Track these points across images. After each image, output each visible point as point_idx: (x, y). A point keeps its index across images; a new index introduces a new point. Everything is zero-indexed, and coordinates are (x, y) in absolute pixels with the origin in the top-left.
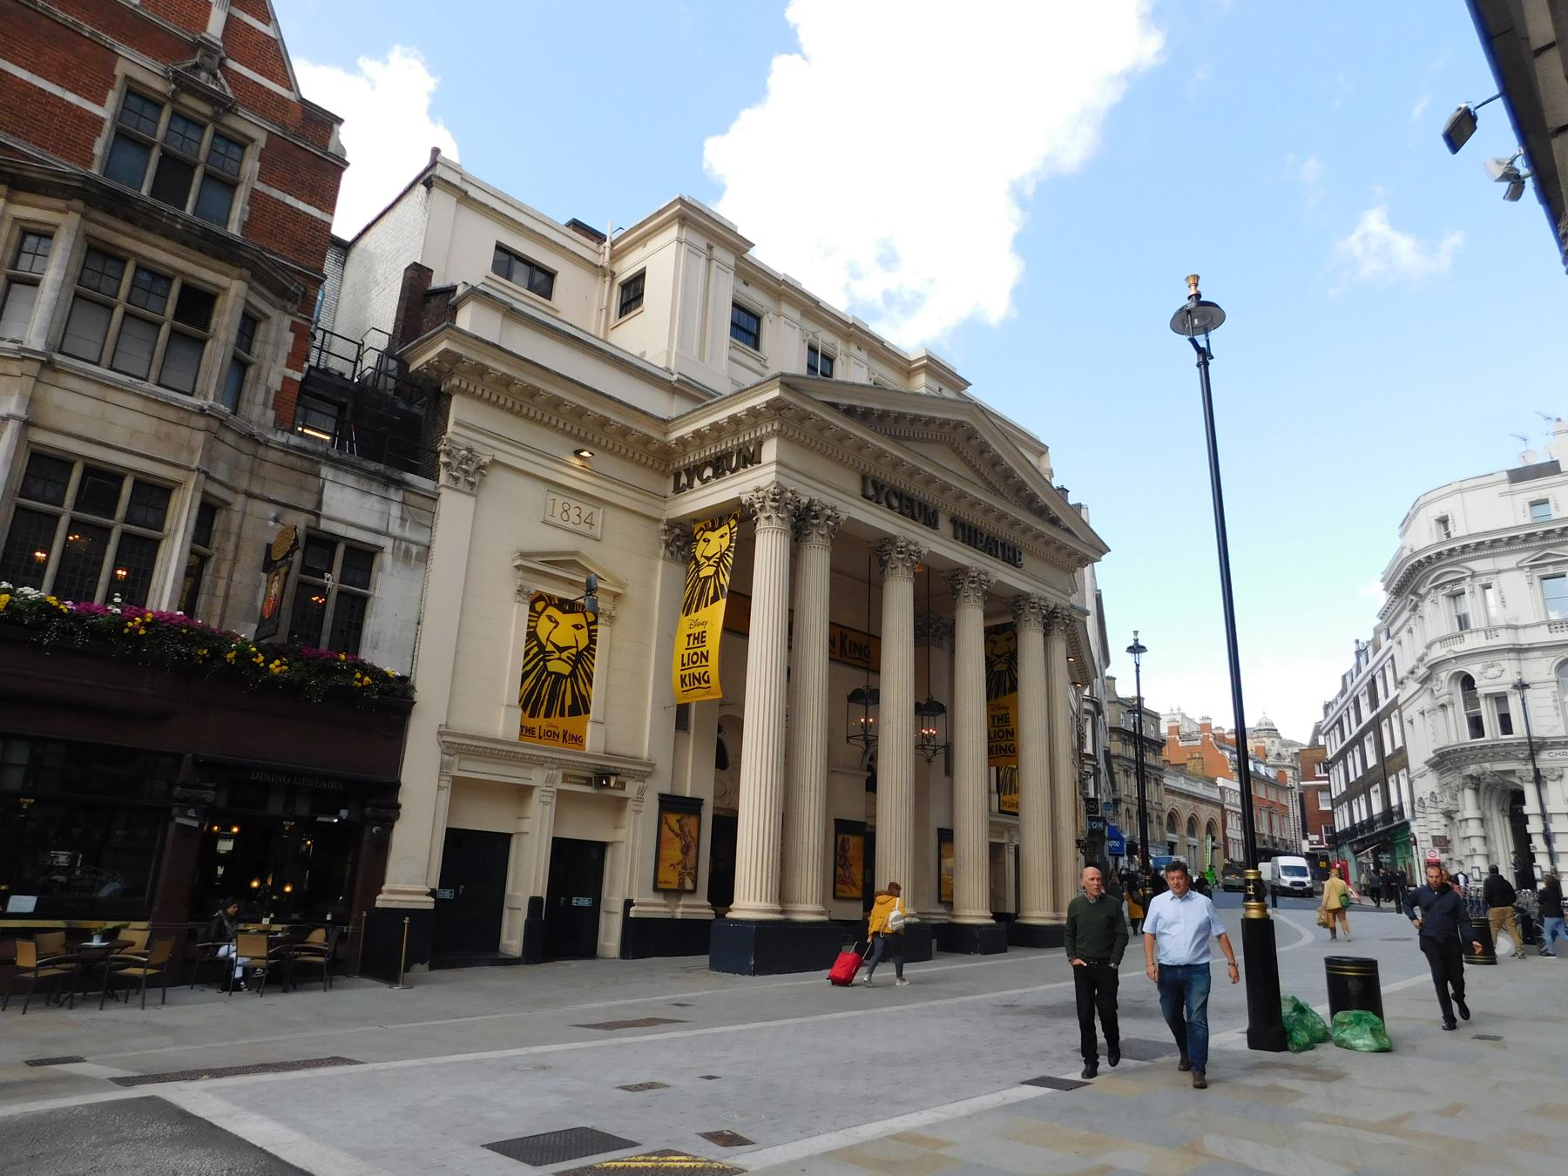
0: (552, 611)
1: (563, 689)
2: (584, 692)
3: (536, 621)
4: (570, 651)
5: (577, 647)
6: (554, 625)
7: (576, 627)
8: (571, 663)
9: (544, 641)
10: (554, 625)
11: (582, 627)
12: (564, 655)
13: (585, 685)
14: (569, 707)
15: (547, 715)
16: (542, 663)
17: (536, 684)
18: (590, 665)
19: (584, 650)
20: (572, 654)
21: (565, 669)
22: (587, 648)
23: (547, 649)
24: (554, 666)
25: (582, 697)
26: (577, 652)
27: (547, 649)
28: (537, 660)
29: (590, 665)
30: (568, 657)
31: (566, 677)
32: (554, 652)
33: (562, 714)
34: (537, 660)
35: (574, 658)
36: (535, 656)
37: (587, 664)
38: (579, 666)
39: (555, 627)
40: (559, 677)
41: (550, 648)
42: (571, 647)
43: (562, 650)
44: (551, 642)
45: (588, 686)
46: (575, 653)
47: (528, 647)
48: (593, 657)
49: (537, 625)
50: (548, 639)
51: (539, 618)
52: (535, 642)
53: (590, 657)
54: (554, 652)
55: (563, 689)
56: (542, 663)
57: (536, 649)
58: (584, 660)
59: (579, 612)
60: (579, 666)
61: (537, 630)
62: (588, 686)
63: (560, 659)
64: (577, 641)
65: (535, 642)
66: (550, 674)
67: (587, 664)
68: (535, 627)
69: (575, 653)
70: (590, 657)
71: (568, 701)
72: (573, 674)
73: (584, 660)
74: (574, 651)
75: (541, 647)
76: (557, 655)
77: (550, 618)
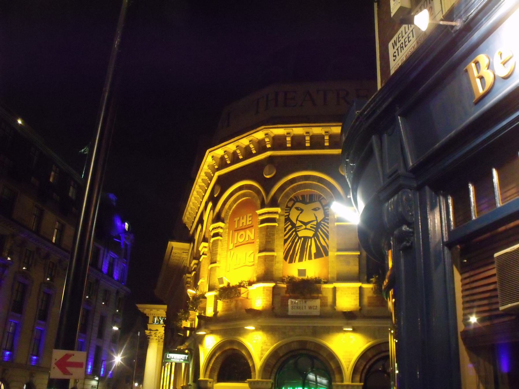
0: (298, 205)
1: (309, 244)
2: (323, 243)
3: (289, 212)
4: (312, 223)
5: (317, 220)
6: (301, 211)
7: (315, 209)
8: (313, 229)
9: (294, 221)
10: (301, 211)
11: (319, 209)
12: (308, 226)
13: (324, 240)
14: (315, 254)
15: (301, 260)
16: (294, 233)
17: (292, 245)
18: (326, 228)
19: (321, 221)
20: (314, 225)
21: (310, 234)
22: (324, 220)
23: (297, 225)
24: (300, 234)
25: (323, 247)
26: (317, 223)
27: (297, 225)
28: (291, 232)
29: (326, 228)
30: (311, 227)
31: (311, 238)
32: (302, 226)
33: (310, 258)
34: (291, 232)
35: (315, 227)
36: (290, 230)
37: (324, 228)
38: (319, 230)
39: (301, 213)
40: (306, 238)
41: (299, 224)
42: (314, 221)
43: (306, 224)
44: (300, 221)
45: (326, 240)
46: (315, 224)
47: (286, 226)
48: (328, 223)
49: (289, 214)
50: (297, 220)
51: (290, 210)
52: (289, 223)
53: (326, 224)
54: (302, 226)
55: (309, 244)
56: (294, 233)
57: (290, 227)
58: (323, 227)
59: (316, 201)
60: (319, 230)
61: (290, 216)
62: (326, 240)
63: (306, 229)
64: (316, 218)
65: (289, 223)
66: (300, 238)
67: (324, 228)
68: (288, 216)
69: (315, 224)
70: (326, 224)
71: (314, 250)
72: (316, 235)
73: (323, 227)
74: (315, 223)
75: (293, 225)
76: (304, 227)
77: (297, 209)
